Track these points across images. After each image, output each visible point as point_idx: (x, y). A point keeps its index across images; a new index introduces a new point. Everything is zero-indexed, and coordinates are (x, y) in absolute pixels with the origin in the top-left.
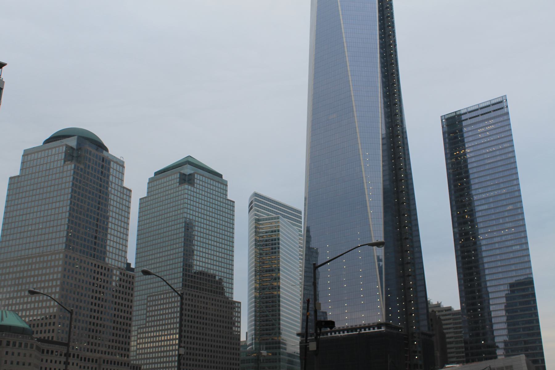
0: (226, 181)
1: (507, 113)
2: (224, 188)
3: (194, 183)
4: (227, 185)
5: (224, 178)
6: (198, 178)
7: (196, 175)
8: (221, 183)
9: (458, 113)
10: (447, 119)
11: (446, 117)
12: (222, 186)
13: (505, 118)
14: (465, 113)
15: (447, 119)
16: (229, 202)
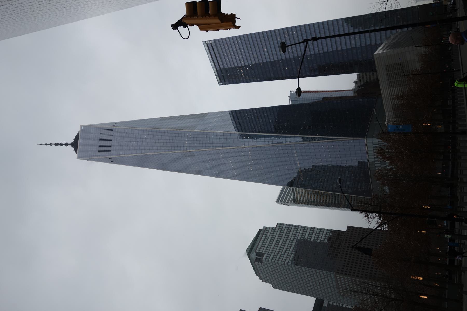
0: (264, 227)
1: (214, 40)
2: (267, 230)
3: (262, 253)
4: (266, 227)
5: (262, 229)
6: (259, 249)
7: (257, 251)
8: (264, 232)
9: (216, 74)
10: (221, 82)
11: (219, 81)
12: (266, 231)
13: (217, 42)
14: (216, 69)
15: (221, 82)
16: (278, 227)
